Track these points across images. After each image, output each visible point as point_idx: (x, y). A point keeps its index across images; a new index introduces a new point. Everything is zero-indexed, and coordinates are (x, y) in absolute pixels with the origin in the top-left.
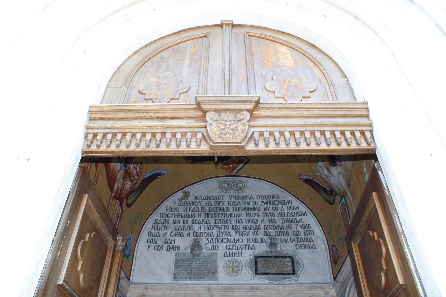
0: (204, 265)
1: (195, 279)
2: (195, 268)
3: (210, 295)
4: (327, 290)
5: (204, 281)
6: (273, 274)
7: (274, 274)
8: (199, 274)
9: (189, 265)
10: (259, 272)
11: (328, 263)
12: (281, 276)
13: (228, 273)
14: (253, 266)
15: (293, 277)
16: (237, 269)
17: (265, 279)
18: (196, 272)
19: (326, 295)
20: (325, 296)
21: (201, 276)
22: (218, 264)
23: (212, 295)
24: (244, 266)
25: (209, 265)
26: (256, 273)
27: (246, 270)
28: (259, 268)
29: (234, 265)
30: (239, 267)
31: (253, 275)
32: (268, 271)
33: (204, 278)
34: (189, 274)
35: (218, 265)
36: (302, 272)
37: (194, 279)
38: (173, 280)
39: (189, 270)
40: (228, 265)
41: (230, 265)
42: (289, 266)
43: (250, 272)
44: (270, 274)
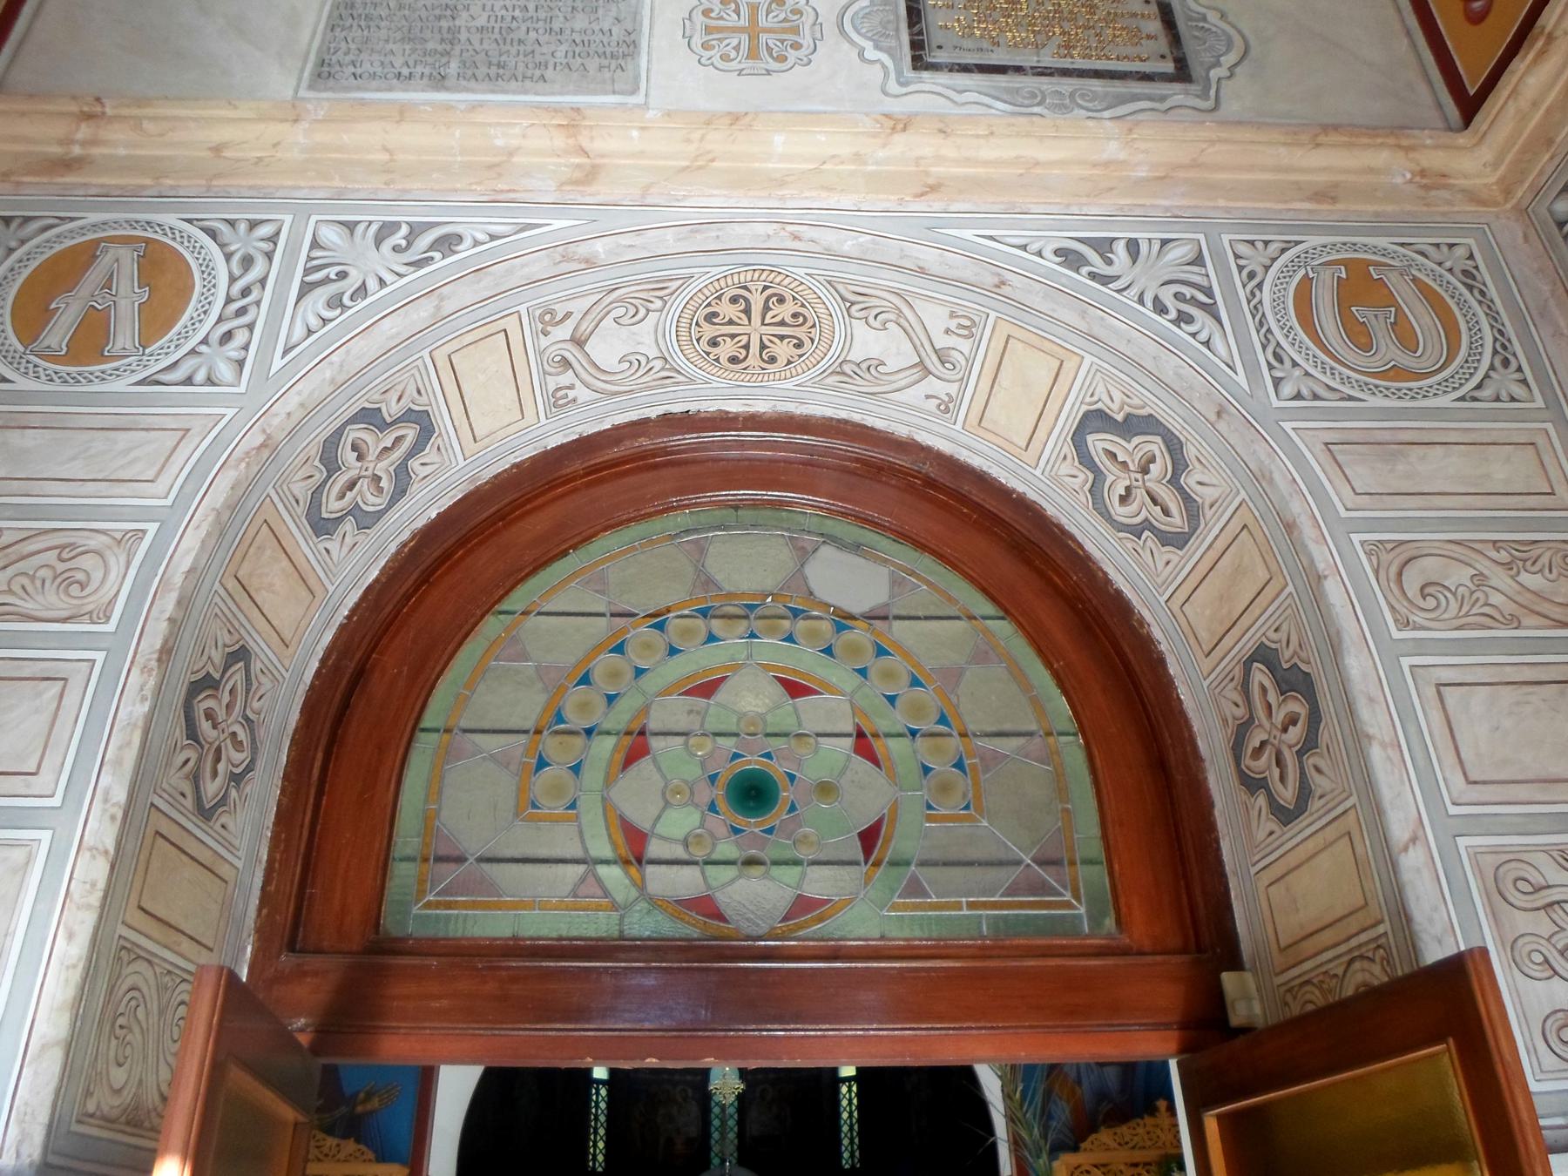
0: (542, 14)
1: (473, 84)
2: (481, 30)
3: (578, 166)
4: (1435, 160)
5: (536, 94)
6: (1034, 74)
7: (1051, 75)
8: (504, 58)
9: (437, 12)
10: (940, 57)
11: (1405, 41)
12: (1096, 85)
13: (717, 60)
14: (897, 30)
15: (1177, 93)
16: (782, 42)
17: (980, 93)
18: (486, 46)
19: (1426, 187)
20: (1422, 193)
21: (521, 66)
22: (646, 12)
23: (594, 166)
24: (830, 29)
25: (579, 15)
26: (919, 63)
27: (846, 46)
28: (936, 37)
29: (762, 21)
30: (796, 30)
31: (899, 73)
32: (996, 58)
33: (543, 77)
34: (430, 60)
35: (646, 23)
36: (1238, 70)
37: (464, 83)
38: (311, 87)
39: (438, 37)
40: (721, 18)
41: (731, 20)
42: (1149, 37)
43: (871, 54)
44: (1019, 70)
